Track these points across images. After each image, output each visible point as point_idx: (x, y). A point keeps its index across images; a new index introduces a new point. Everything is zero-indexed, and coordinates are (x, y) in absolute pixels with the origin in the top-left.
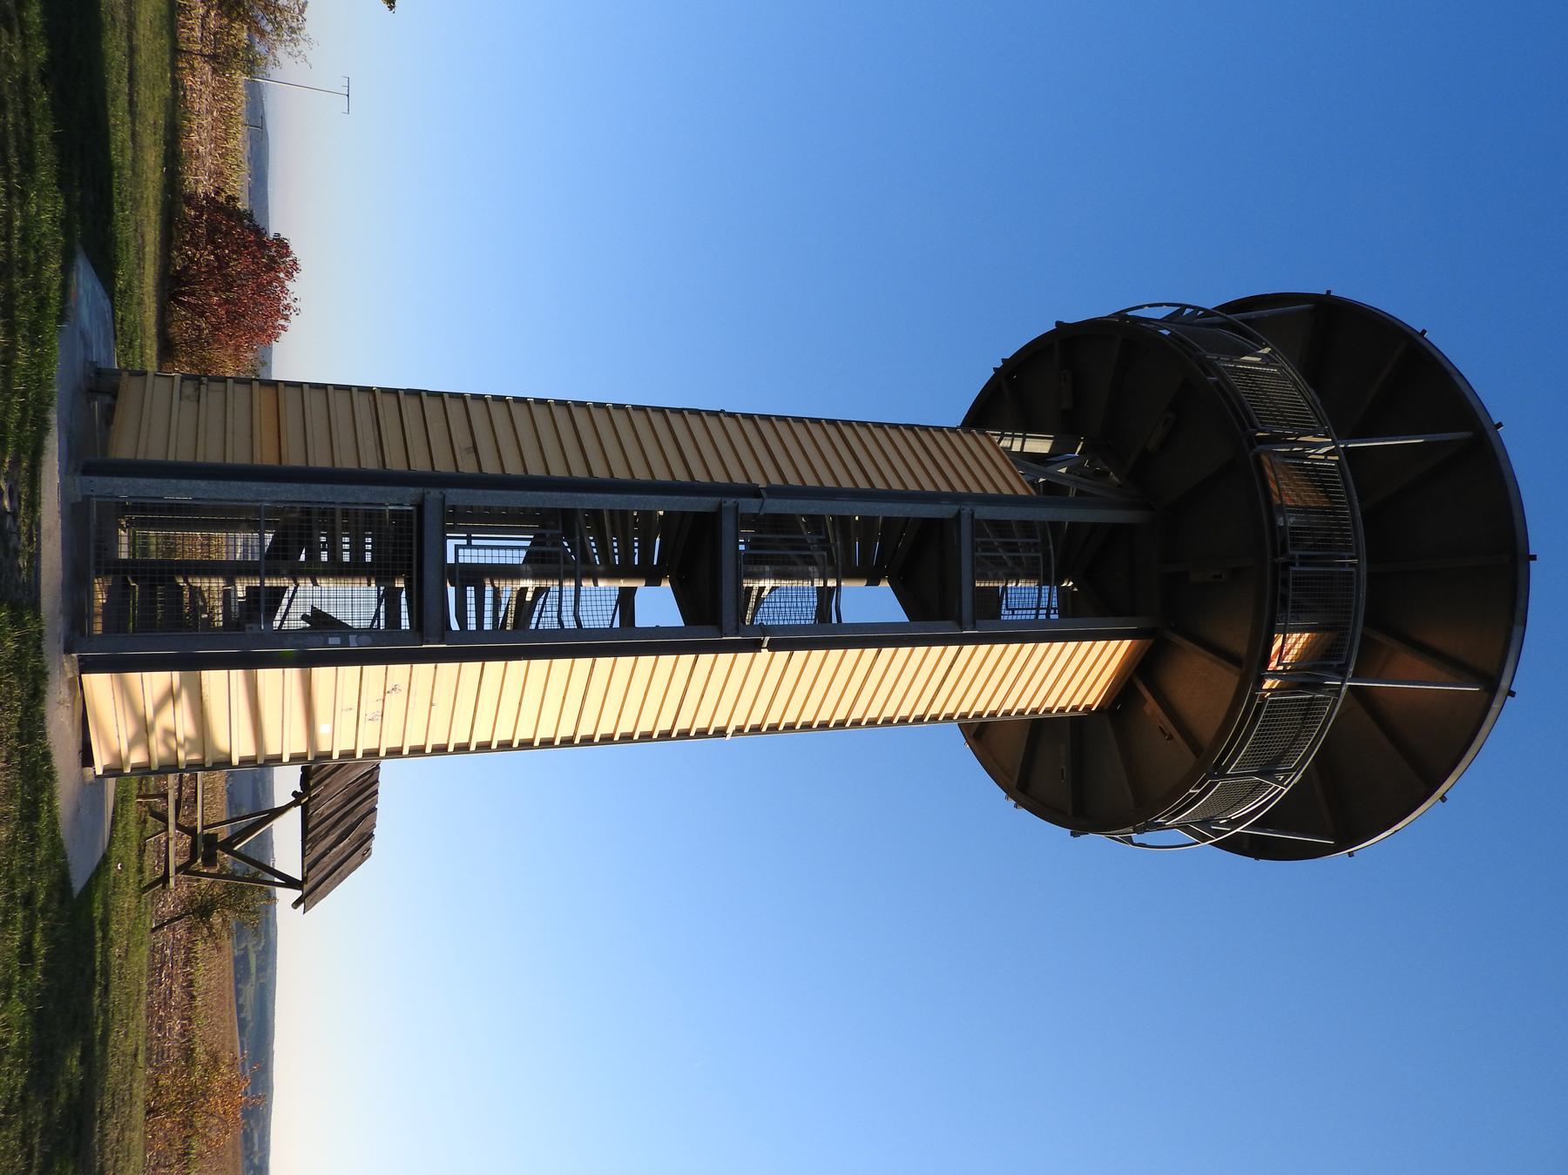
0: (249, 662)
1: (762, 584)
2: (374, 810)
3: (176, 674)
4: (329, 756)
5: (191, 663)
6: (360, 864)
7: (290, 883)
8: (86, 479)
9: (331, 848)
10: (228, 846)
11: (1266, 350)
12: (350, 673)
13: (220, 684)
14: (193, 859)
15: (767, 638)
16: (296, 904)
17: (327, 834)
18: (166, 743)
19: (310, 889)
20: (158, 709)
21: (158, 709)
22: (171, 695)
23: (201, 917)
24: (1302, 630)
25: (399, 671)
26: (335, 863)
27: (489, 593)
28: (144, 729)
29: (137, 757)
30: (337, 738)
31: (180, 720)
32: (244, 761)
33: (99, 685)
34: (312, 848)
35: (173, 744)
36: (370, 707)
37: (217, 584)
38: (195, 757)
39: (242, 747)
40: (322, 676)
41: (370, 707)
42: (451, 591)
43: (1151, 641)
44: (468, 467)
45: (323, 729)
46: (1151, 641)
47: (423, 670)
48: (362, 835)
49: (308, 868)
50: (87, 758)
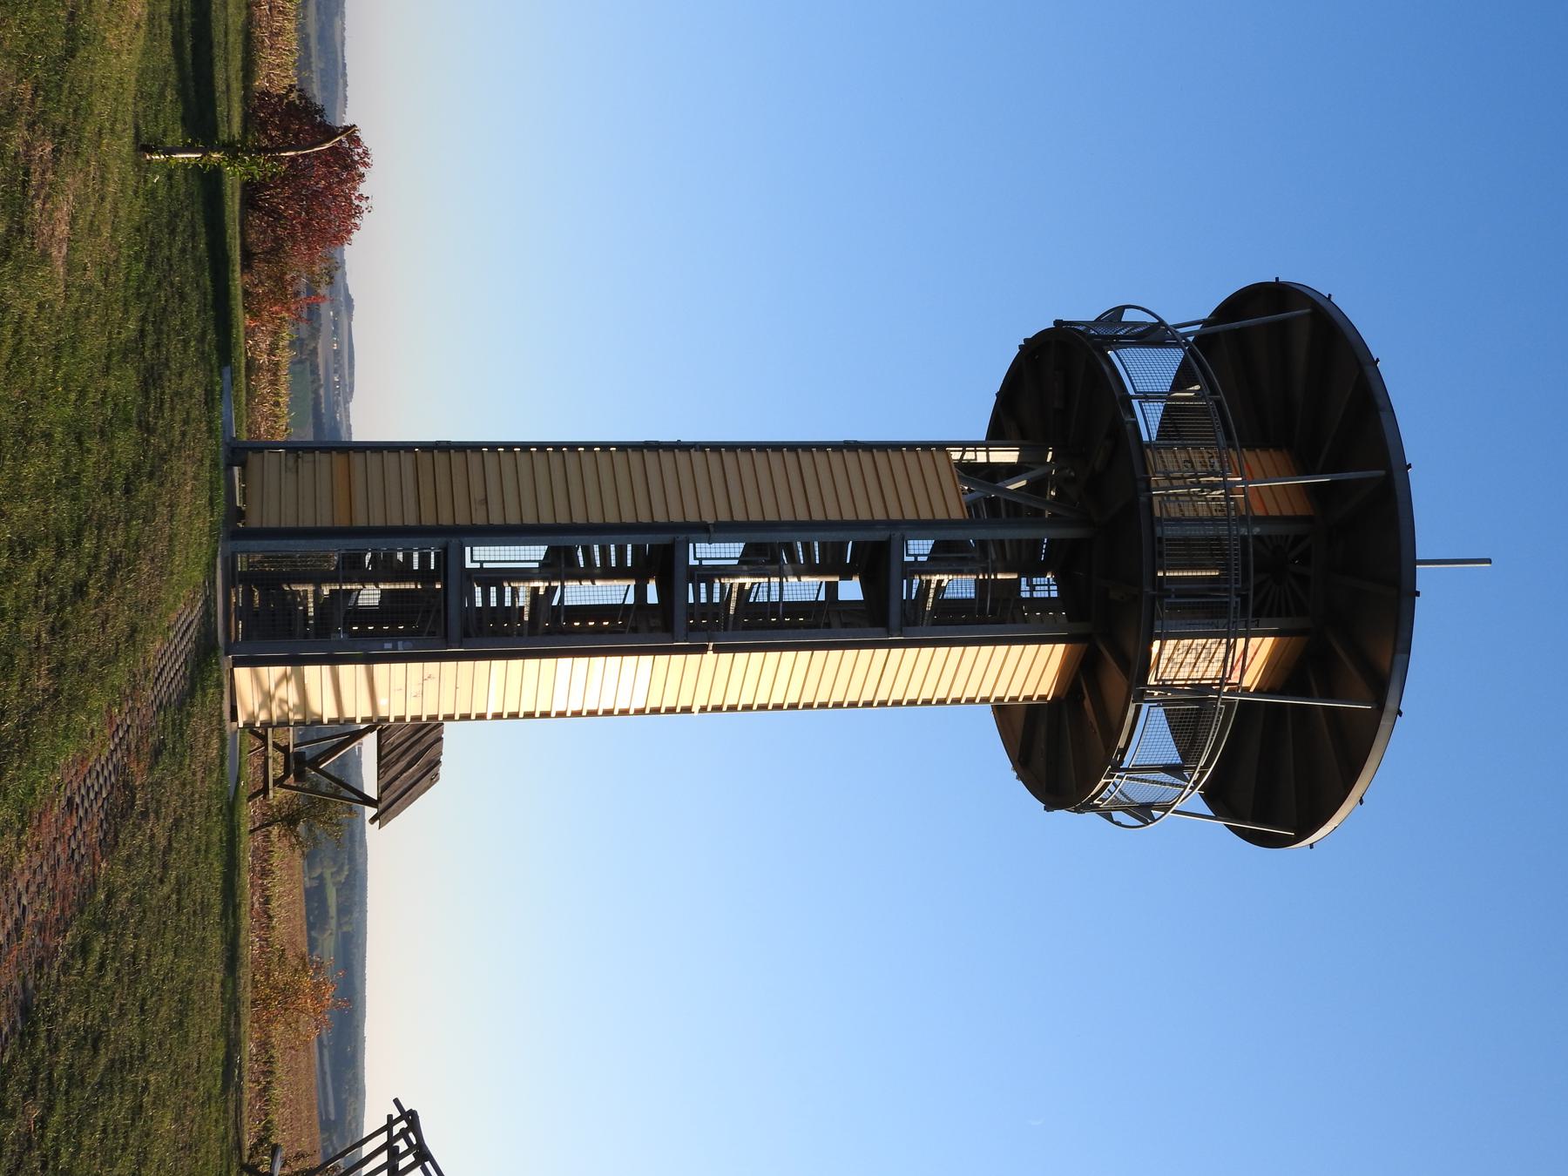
0: (333, 660)
1: (741, 580)
2: (440, 739)
3: (289, 668)
4: (387, 719)
5: (297, 661)
6: (428, 787)
7: (369, 801)
8: (234, 542)
9: (401, 773)
10: (315, 763)
11: (1197, 387)
12: (399, 668)
13: (315, 674)
14: (286, 776)
15: (712, 644)
16: (373, 820)
17: (398, 761)
18: (280, 707)
19: (387, 808)
20: (277, 685)
21: (277, 685)
22: (285, 677)
23: (289, 825)
24: (1264, 634)
25: (432, 667)
26: (405, 786)
27: (508, 590)
28: (268, 697)
29: (263, 716)
30: (392, 707)
31: (289, 693)
32: (331, 721)
33: (243, 675)
34: (385, 772)
35: (286, 708)
36: (414, 688)
37: (310, 588)
38: (298, 717)
39: (329, 713)
40: (380, 669)
41: (414, 688)
42: (478, 590)
43: (1086, 645)
44: (479, 519)
45: (382, 702)
46: (1086, 645)
47: (449, 666)
48: (430, 762)
49: (382, 789)
50: (234, 717)
